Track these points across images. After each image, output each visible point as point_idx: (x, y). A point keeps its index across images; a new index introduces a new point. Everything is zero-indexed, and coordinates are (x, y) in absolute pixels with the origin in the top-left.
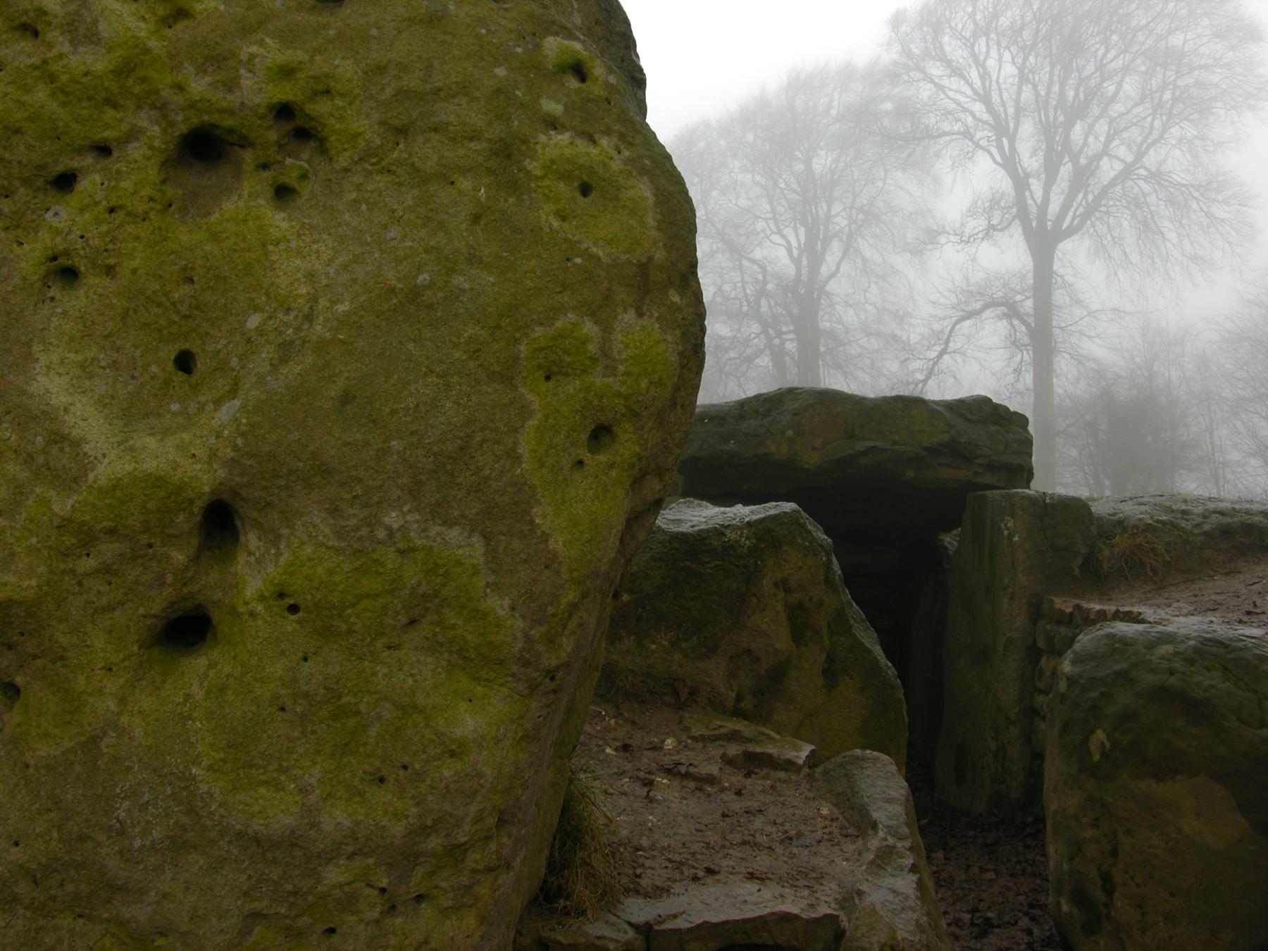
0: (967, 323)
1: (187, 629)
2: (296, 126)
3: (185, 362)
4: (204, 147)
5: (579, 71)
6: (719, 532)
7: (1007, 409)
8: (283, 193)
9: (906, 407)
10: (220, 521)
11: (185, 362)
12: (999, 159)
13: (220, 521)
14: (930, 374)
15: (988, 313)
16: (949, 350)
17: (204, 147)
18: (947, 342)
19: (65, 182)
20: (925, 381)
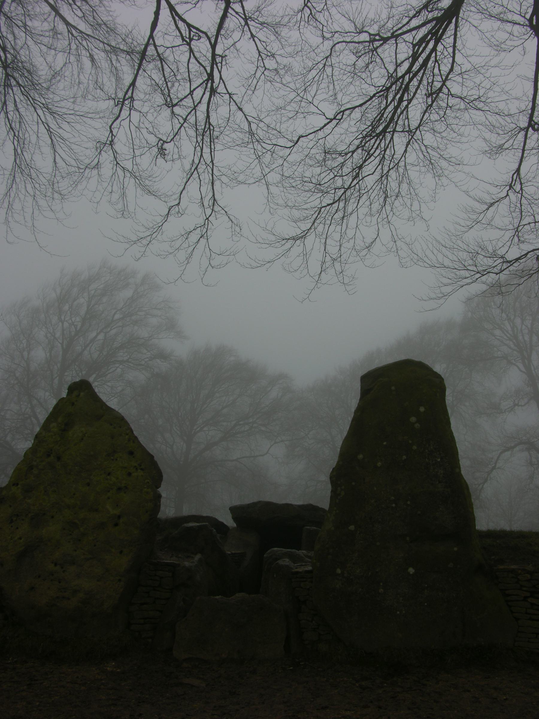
0: (506, 453)
1: (116, 525)
2: (126, 487)
3: (117, 505)
4: (119, 489)
5: (148, 483)
6: (192, 527)
7: (318, 507)
8: (125, 493)
9: (288, 506)
10: (119, 517)
11: (117, 505)
12: (524, 370)
13: (119, 517)
14: (486, 480)
15: (517, 448)
16: (497, 466)
17: (119, 489)
18: (496, 463)
19: (109, 491)
20: (484, 483)
